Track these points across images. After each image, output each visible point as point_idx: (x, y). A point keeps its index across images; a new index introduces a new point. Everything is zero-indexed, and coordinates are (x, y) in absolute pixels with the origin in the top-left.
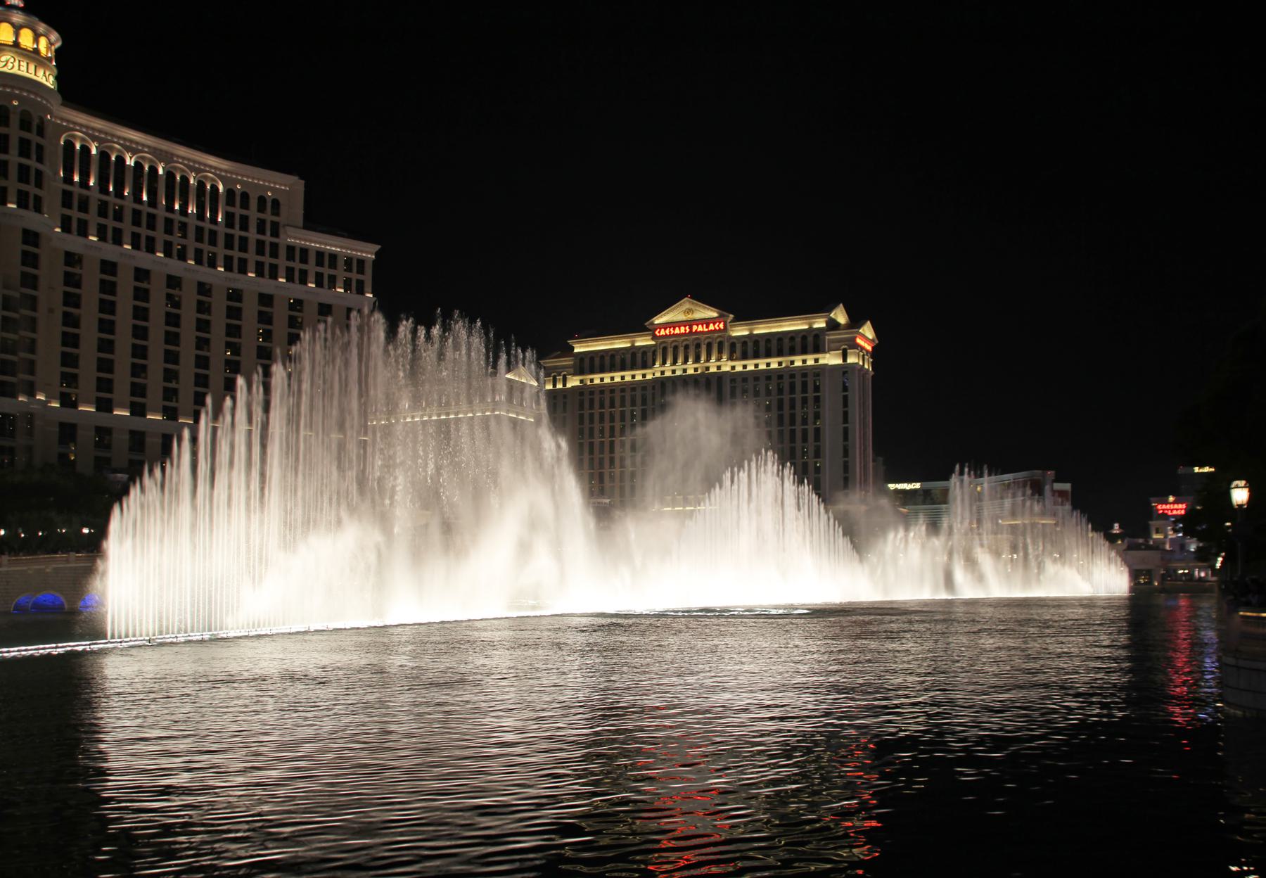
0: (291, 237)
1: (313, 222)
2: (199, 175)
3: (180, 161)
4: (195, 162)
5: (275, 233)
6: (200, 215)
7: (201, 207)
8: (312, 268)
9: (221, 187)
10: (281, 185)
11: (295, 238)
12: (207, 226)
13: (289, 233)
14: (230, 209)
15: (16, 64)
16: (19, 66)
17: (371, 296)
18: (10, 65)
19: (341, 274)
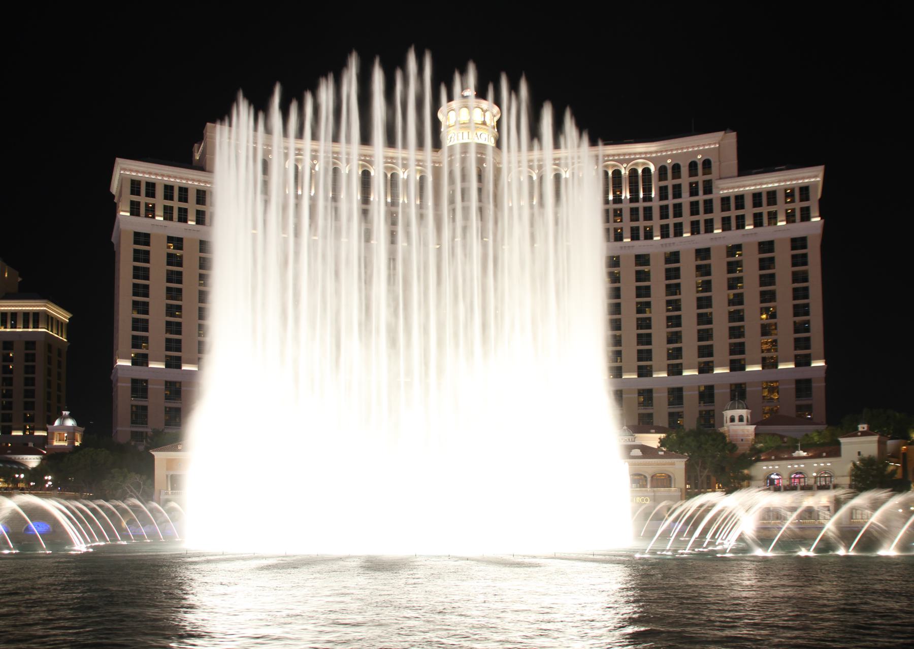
0: (723, 189)
1: (747, 166)
2: (629, 165)
3: (611, 158)
4: (624, 155)
5: (708, 189)
6: (634, 198)
7: (634, 191)
8: (749, 211)
9: (652, 168)
10: (710, 144)
11: (728, 189)
12: (641, 205)
13: (721, 186)
14: (663, 183)
15: (456, 137)
16: (458, 136)
17: (818, 219)
18: (452, 139)
19: (781, 207)
